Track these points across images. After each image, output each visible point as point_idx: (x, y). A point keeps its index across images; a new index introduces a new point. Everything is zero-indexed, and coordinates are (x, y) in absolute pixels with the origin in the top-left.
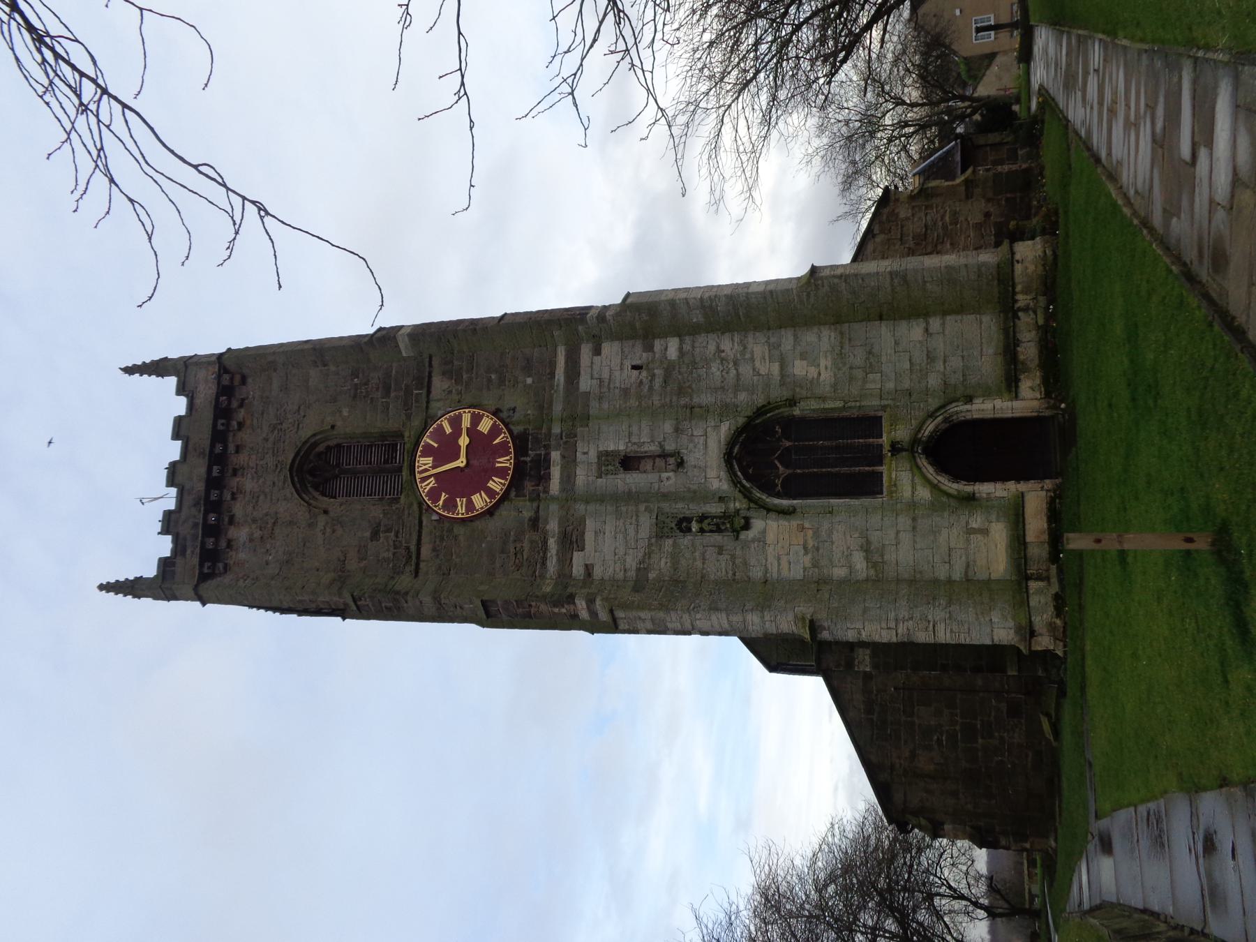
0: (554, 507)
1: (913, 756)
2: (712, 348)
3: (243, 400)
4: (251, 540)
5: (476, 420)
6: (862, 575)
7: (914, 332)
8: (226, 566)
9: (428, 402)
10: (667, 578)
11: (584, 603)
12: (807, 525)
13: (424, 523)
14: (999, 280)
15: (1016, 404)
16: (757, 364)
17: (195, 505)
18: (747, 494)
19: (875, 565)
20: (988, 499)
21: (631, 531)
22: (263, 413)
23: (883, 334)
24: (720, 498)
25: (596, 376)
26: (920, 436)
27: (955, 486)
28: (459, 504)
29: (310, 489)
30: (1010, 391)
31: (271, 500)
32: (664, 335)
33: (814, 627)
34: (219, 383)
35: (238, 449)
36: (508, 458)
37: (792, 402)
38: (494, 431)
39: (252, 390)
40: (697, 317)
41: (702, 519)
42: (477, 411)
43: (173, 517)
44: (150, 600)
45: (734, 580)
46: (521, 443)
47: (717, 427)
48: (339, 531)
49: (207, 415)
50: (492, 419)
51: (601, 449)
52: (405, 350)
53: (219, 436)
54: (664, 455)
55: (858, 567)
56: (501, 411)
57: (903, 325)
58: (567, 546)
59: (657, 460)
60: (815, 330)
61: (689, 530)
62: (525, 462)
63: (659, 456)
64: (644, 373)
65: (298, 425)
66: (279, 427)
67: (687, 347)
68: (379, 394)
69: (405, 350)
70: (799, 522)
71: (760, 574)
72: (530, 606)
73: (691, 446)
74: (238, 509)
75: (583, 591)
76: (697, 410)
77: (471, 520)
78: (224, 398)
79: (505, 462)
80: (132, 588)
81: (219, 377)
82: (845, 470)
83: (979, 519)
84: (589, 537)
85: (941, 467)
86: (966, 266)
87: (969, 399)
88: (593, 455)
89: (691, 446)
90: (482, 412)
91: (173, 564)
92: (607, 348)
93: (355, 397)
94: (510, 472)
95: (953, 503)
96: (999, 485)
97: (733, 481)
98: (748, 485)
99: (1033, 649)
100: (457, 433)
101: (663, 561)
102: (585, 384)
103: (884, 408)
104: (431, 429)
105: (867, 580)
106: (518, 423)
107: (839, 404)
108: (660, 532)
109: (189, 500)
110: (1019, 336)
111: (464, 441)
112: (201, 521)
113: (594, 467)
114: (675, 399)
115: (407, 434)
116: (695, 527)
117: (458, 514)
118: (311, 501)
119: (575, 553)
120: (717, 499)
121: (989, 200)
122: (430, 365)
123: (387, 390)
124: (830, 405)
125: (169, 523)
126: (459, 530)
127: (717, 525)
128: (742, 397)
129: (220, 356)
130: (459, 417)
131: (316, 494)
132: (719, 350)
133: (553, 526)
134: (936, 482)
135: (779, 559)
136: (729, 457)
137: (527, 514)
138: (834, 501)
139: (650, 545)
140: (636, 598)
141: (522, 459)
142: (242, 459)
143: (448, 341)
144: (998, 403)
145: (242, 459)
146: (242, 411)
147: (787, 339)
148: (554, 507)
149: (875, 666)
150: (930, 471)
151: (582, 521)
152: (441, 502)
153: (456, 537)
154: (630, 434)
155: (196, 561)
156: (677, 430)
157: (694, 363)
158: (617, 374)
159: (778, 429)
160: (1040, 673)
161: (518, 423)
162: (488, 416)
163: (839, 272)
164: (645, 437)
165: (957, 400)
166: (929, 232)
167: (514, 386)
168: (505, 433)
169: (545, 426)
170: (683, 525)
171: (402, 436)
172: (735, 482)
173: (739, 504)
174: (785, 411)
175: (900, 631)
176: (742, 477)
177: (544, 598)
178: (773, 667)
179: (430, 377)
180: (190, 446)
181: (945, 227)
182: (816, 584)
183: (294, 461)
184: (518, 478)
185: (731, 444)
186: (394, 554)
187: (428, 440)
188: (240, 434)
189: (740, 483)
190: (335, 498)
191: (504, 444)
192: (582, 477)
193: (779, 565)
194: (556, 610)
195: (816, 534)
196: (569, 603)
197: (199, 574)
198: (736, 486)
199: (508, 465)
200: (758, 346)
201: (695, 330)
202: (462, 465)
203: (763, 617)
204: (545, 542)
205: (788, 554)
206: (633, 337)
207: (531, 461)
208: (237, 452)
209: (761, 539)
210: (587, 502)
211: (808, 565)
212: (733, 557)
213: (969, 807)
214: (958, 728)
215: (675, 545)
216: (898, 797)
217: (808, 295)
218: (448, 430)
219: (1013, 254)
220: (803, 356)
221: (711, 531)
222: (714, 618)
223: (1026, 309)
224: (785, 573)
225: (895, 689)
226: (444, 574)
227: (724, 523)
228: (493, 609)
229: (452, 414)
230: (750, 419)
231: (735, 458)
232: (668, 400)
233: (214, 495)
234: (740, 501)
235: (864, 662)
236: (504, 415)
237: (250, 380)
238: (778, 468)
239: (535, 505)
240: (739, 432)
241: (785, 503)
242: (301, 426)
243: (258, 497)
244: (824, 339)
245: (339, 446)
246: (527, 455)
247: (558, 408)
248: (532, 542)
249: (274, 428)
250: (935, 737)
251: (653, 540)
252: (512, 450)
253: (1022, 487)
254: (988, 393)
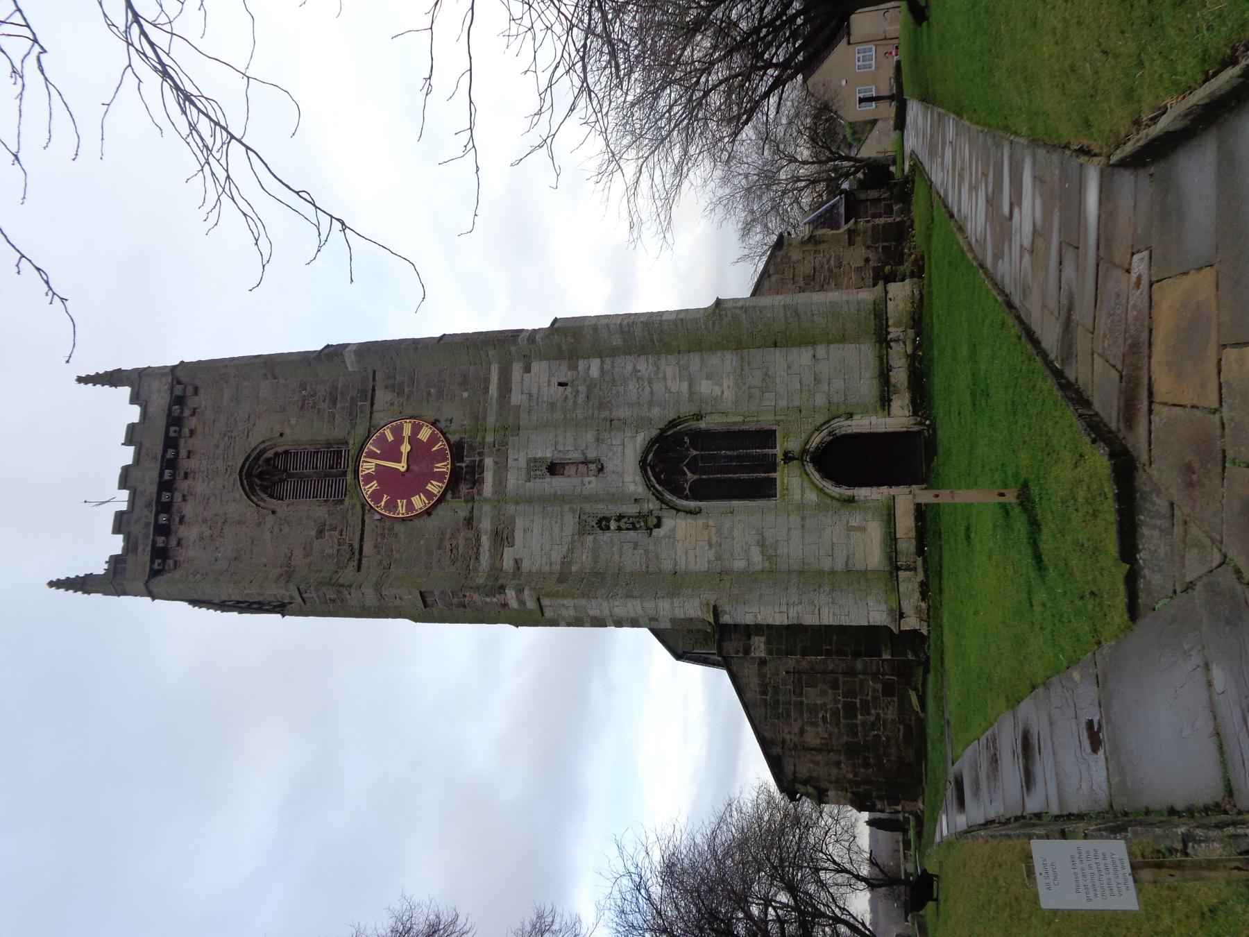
0: (487, 508)
1: (802, 732)
2: (629, 368)
3: (195, 409)
4: (201, 539)
5: (416, 429)
6: (759, 567)
7: (803, 357)
8: (176, 562)
9: (371, 413)
10: (587, 571)
11: (513, 593)
12: (711, 523)
13: (366, 522)
14: (875, 315)
15: (888, 420)
16: (669, 382)
17: (146, 507)
18: (660, 498)
19: (769, 558)
20: (866, 501)
21: (557, 529)
22: (214, 422)
23: (778, 359)
24: (636, 500)
25: (526, 391)
26: (808, 447)
27: (838, 490)
28: (400, 504)
29: (259, 492)
30: (884, 410)
31: (221, 501)
32: (588, 356)
33: (716, 612)
34: (171, 394)
35: (189, 455)
36: (445, 463)
37: (699, 416)
38: (433, 440)
39: (203, 401)
40: (617, 341)
41: (620, 518)
42: (417, 421)
43: (125, 517)
44: (99, 595)
45: (647, 572)
46: (457, 451)
47: (633, 438)
48: (286, 529)
49: (160, 423)
50: (431, 428)
51: (530, 456)
52: (351, 365)
53: (171, 443)
54: (586, 463)
55: (756, 559)
56: (439, 421)
57: (794, 352)
58: (499, 542)
59: (580, 466)
60: (719, 354)
61: (608, 528)
62: (461, 468)
63: (582, 463)
64: (569, 389)
65: (248, 432)
66: (229, 434)
67: (607, 367)
68: (326, 405)
69: (351, 365)
70: (705, 521)
71: (670, 567)
72: (465, 596)
73: (610, 454)
74: (189, 510)
75: (513, 582)
76: (615, 422)
77: (410, 519)
78: (177, 407)
79: (443, 467)
80: (83, 584)
81: (172, 387)
82: (744, 476)
83: (857, 519)
84: (518, 534)
85: (826, 473)
86: (847, 302)
87: (850, 416)
88: (522, 462)
89: (610, 454)
90: (422, 422)
91: (124, 561)
92: (537, 366)
93: (302, 408)
94: (447, 476)
95: (835, 503)
96: (875, 490)
97: (647, 485)
98: (660, 488)
99: (902, 629)
100: (399, 440)
101: (584, 557)
102: (516, 398)
103: (778, 423)
104: (374, 437)
105: (763, 571)
106: (455, 432)
107: (740, 419)
108: (582, 530)
109: (141, 501)
110: (891, 363)
111: (405, 448)
112: (153, 522)
113: (524, 471)
114: (596, 412)
115: (351, 442)
116: (613, 525)
117: (398, 514)
118: (259, 503)
119: (506, 549)
120: (633, 501)
121: (868, 248)
122: (374, 379)
123: (334, 402)
124: (731, 419)
125: (121, 523)
126: (399, 528)
127: (633, 524)
128: (656, 411)
129: (173, 368)
130: (401, 428)
131: (264, 496)
132: (636, 371)
133: (486, 525)
134: (821, 486)
135: (686, 554)
136: (643, 464)
137: (463, 512)
138: (735, 503)
139: (573, 542)
140: (562, 587)
141: (458, 464)
142: (192, 464)
143: (392, 359)
144: (874, 419)
145: (192, 464)
146: (194, 419)
147: (694, 361)
148: (487, 508)
149: (770, 652)
150: (816, 476)
151: (512, 520)
152: (383, 503)
153: (396, 535)
154: (556, 443)
155: (147, 558)
156: (598, 440)
157: (614, 380)
158: (545, 389)
159: (687, 439)
160: (910, 657)
161: (455, 432)
162: (427, 426)
163: (740, 304)
164: (568, 446)
165: (839, 417)
166: (817, 273)
167: (451, 399)
168: (442, 441)
169: (479, 435)
170: (603, 523)
171: (347, 443)
172: (649, 486)
173: (652, 505)
174: (693, 425)
175: (790, 615)
176: (655, 481)
177: (477, 589)
178: (679, 656)
179: (374, 390)
180: (143, 452)
181: (830, 270)
182: (720, 576)
183: (244, 464)
184: (454, 481)
185: (646, 452)
186: (338, 550)
187: (371, 447)
188: (191, 441)
189: (654, 487)
190: (282, 500)
191: (441, 451)
192: (513, 480)
193: (687, 558)
194: (488, 600)
195: (719, 531)
196: (500, 593)
197: (150, 571)
198: (650, 490)
199: (445, 470)
200: (669, 366)
201: (614, 353)
202: (403, 470)
203: (672, 604)
204: (478, 539)
205: (695, 549)
206: (559, 357)
207: (466, 467)
208: (188, 457)
209: (671, 536)
210: (517, 503)
211: (712, 558)
212: (646, 551)
213: (850, 776)
214: (840, 706)
215: (595, 540)
216: (789, 768)
217: (714, 323)
218: (390, 438)
219: (886, 292)
220: (708, 377)
221: (628, 529)
222: (630, 604)
223: (897, 340)
224: (692, 566)
225: (786, 672)
226: (384, 569)
227: (639, 522)
228: (429, 600)
229: (394, 424)
230: (663, 431)
231: (649, 465)
232: (590, 413)
233: (165, 497)
234: (653, 503)
235: (759, 646)
236: (442, 425)
237: (201, 391)
238: (686, 474)
239: (470, 505)
240: (653, 442)
241: (693, 504)
242: (251, 433)
243: (208, 499)
244: (726, 362)
245: (286, 452)
246: (462, 461)
247: (491, 420)
248: (467, 539)
249: (225, 435)
250: (821, 715)
251: (576, 537)
252: (449, 456)
253: (894, 490)
254: (865, 411)
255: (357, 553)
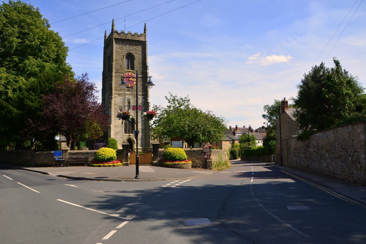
21: (120, 103)
47: (133, 114)
84: (120, 97)
133: (121, 92)
151: (122, 96)
191: (132, 85)
192: (127, 96)
204: (119, 91)
255: (117, 72)
